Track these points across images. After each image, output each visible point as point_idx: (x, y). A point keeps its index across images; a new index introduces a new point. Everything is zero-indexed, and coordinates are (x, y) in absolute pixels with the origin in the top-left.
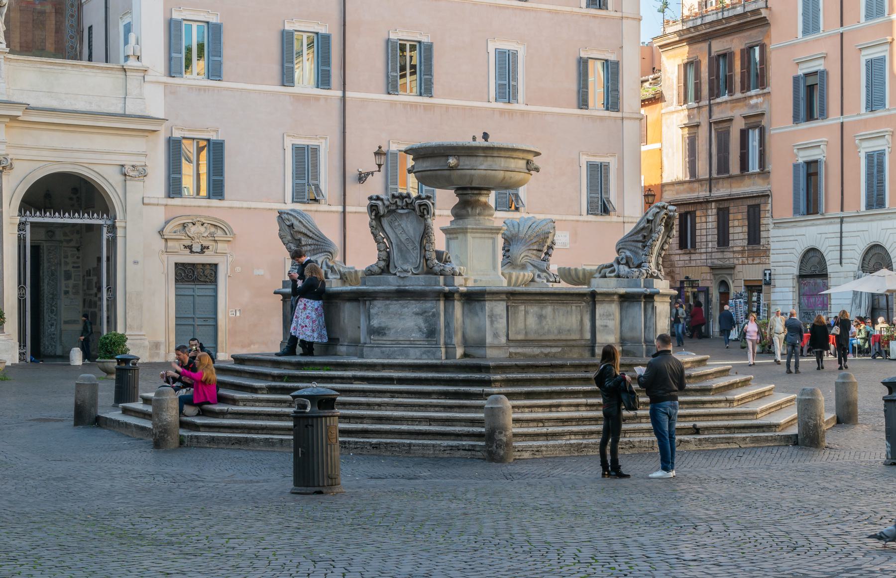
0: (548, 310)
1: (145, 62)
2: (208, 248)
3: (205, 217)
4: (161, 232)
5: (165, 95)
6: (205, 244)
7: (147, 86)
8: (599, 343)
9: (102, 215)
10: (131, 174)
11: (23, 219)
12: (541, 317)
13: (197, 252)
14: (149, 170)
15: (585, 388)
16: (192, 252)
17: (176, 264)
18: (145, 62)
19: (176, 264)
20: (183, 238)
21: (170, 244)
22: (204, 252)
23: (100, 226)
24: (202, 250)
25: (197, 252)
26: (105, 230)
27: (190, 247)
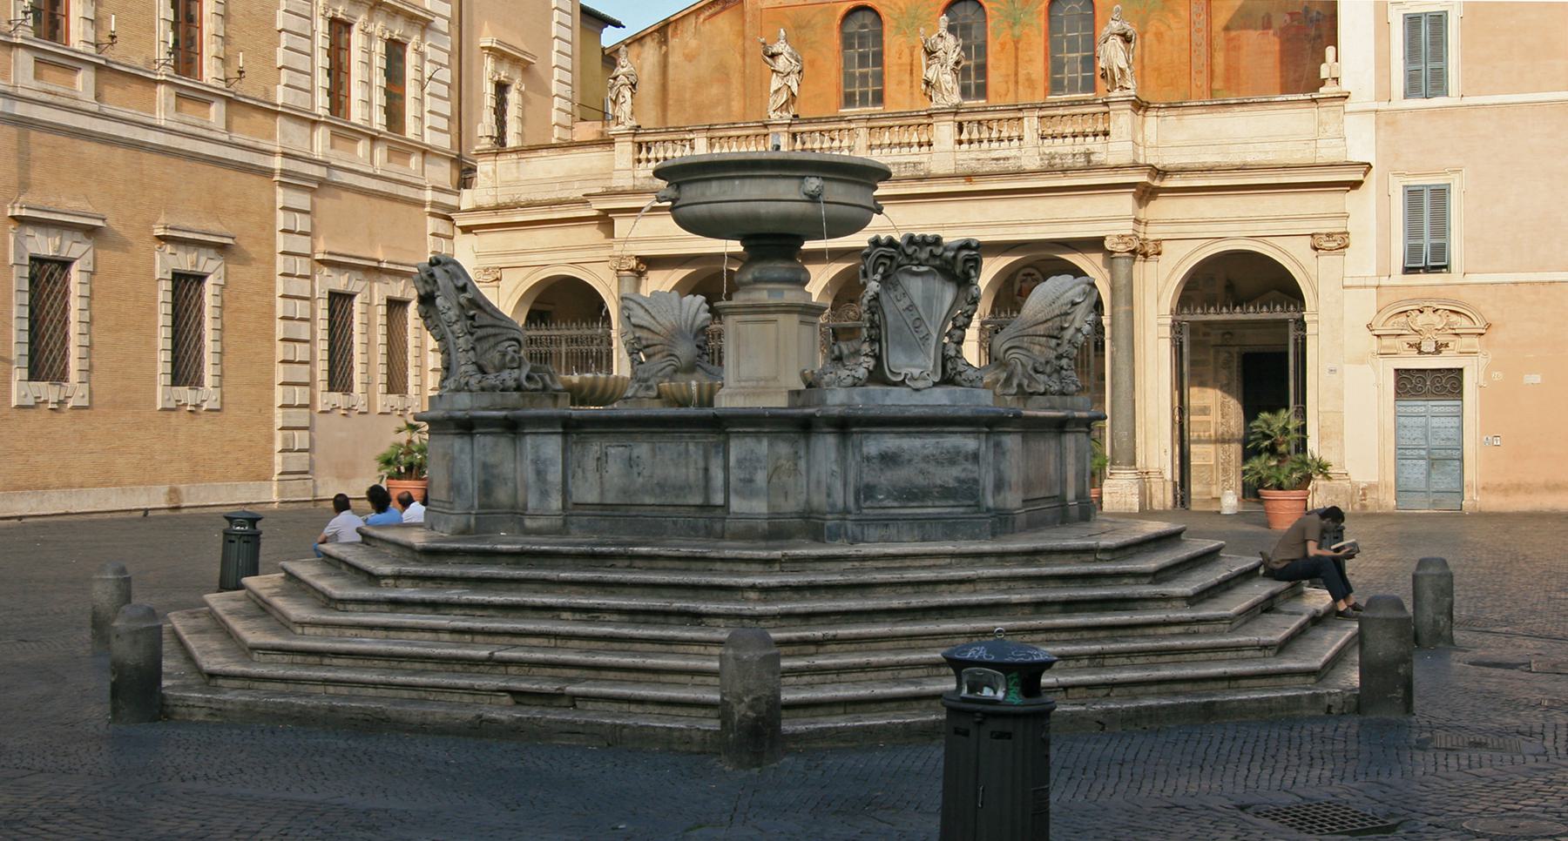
0: (642, 450)
1: (1345, 86)
2: (1447, 345)
3: (1438, 300)
4: (1369, 326)
5: (1377, 129)
6: (1442, 340)
7: (1346, 117)
8: (734, 513)
9: (1288, 307)
10: (1326, 245)
11: (1180, 318)
12: (631, 462)
13: (1428, 353)
14: (1353, 240)
15: (492, 599)
16: (1420, 352)
17: (1397, 370)
18: (1345, 86)
19: (1397, 370)
20: (1406, 332)
21: (1386, 341)
22: (1440, 352)
23: (1285, 322)
24: (1436, 348)
25: (1428, 353)
26: (1292, 327)
27: (1418, 347)
